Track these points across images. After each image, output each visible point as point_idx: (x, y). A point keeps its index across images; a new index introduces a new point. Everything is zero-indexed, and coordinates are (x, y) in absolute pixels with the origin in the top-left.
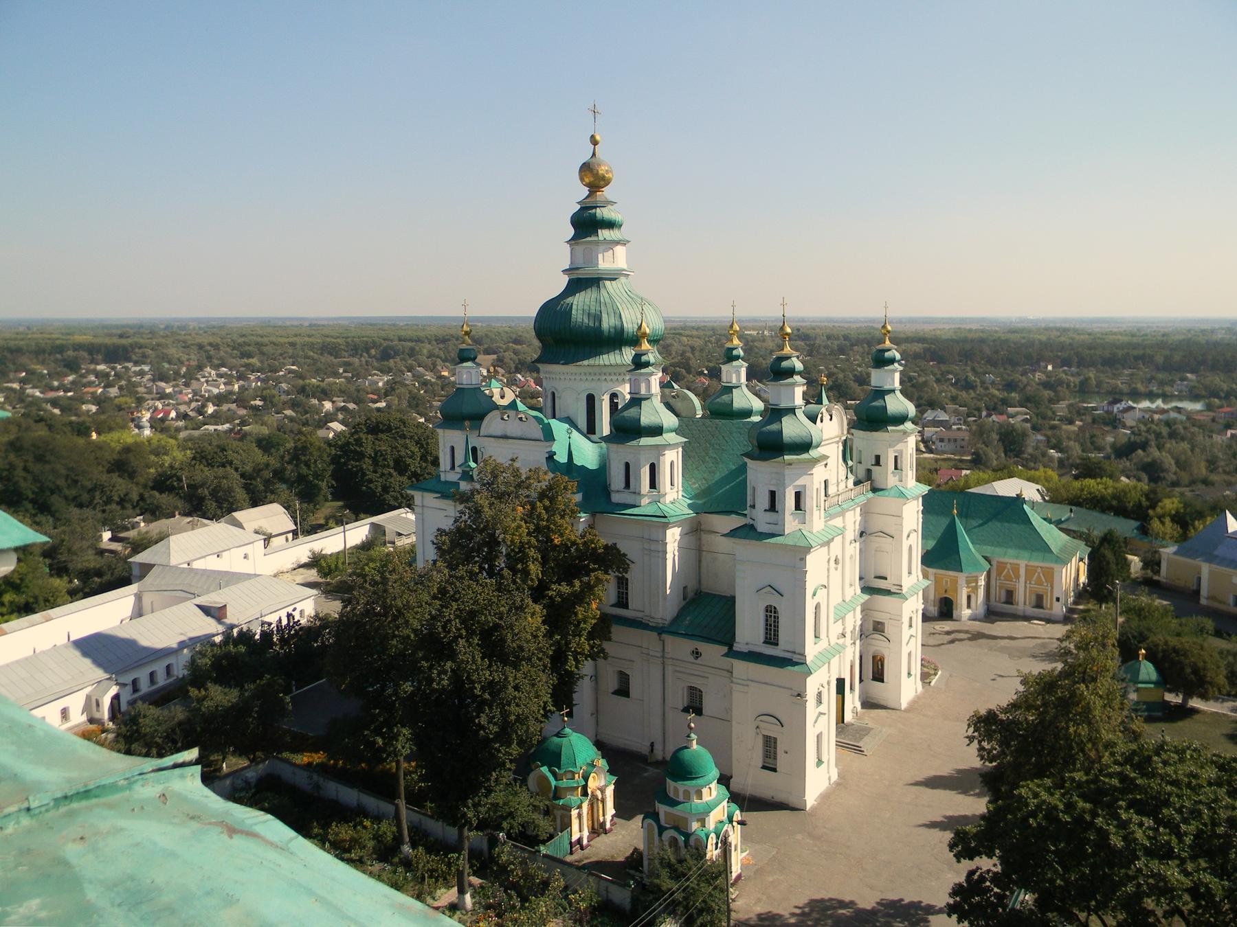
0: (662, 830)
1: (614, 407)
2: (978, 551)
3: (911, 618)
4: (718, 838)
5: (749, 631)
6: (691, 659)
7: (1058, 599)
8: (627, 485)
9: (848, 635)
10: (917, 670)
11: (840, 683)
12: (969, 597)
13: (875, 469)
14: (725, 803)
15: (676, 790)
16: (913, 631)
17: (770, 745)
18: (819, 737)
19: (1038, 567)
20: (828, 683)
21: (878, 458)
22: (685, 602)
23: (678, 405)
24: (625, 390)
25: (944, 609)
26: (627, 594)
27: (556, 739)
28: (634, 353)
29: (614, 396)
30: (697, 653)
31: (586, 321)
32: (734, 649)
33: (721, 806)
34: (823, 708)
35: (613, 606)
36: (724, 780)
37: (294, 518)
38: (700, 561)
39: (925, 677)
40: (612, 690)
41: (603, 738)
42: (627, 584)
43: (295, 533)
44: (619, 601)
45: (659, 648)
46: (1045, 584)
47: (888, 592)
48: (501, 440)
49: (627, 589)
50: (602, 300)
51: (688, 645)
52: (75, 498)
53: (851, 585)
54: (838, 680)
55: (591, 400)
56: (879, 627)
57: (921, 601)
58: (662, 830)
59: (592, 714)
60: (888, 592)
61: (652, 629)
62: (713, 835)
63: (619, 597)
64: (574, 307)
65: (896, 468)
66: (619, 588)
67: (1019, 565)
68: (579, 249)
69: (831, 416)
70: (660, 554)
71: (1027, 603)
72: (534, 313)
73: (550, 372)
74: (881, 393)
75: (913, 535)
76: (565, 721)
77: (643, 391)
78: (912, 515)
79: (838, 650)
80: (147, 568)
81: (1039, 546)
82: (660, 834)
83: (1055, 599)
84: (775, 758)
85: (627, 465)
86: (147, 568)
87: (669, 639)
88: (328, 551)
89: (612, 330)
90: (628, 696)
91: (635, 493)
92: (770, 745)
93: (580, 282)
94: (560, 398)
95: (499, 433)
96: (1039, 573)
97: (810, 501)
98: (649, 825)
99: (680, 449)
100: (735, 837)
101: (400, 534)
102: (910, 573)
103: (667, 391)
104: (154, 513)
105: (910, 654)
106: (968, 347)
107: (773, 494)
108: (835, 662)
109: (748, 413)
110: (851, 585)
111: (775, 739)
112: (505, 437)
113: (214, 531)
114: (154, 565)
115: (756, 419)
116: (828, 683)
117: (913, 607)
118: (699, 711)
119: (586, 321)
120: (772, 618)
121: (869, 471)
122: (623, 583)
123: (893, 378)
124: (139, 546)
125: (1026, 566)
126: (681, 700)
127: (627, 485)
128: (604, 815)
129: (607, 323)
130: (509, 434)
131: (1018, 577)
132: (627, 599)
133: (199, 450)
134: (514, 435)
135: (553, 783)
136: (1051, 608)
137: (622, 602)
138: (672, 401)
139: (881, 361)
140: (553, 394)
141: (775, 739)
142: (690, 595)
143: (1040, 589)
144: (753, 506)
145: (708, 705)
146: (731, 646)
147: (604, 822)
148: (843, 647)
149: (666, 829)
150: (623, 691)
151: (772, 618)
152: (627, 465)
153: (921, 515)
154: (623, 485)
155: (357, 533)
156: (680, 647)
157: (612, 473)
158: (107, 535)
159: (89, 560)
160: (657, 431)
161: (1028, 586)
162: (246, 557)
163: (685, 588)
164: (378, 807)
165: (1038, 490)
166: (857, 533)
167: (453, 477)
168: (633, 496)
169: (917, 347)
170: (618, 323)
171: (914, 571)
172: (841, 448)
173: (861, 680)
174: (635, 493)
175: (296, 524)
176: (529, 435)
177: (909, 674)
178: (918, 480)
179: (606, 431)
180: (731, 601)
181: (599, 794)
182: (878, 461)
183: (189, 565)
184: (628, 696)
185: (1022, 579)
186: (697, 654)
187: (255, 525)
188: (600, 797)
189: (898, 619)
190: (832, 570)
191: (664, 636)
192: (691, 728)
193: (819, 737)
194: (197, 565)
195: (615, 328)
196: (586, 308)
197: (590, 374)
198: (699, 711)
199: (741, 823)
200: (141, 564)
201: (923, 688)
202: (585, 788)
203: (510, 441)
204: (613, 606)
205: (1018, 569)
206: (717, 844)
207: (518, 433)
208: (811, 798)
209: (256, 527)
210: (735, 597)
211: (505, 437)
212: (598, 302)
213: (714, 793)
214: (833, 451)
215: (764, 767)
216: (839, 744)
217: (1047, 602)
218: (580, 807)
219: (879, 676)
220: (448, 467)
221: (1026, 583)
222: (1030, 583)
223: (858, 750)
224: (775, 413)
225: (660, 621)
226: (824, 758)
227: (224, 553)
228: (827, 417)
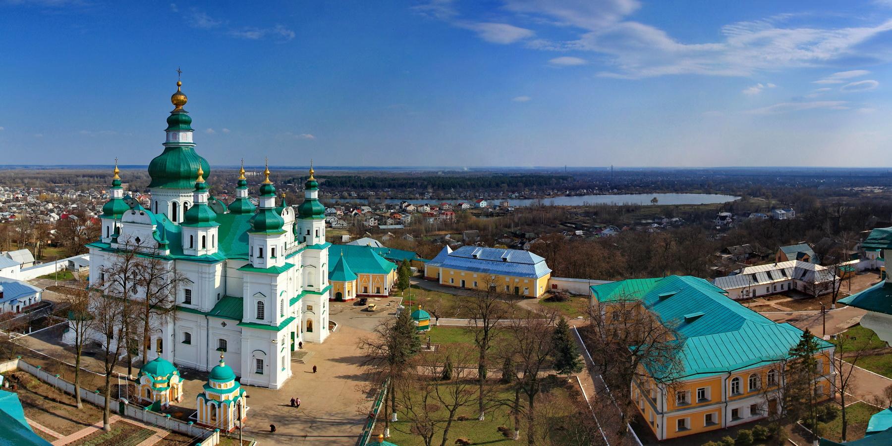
0: (207, 401)
1: (185, 208)
2: (352, 271)
3: (324, 303)
4: (235, 403)
5: (249, 313)
6: (221, 326)
7: (386, 289)
9: (296, 313)
10: (327, 325)
11: (293, 334)
12: (349, 291)
13: (306, 236)
14: (238, 389)
15: (214, 384)
16: (325, 309)
17: (260, 363)
18: (283, 358)
20: (287, 334)
21: (308, 231)
22: (217, 301)
23: (216, 208)
24: (191, 201)
25: (338, 298)
26: (190, 297)
27: (155, 362)
28: (195, 183)
29: (186, 203)
30: (224, 324)
31: (173, 167)
32: (243, 321)
33: (236, 390)
34: (284, 346)
35: (183, 303)
36: (238, 379)
38: (226, 282)
39: (331, 328)
41: (176, 362)
42: (190, 293)
44: (186, 301)
45: (206, 322)
47: (314, 292)
49: (190, 295)
51: (221, 320)
53: (297, 290)
54: (292, 333)
55: (175, 205)
56: (310, 308)
57: (328, 295)
58: (207, 401)
60: (314, 292)
61: (203, 313)
62: (233, 402)
63: (186, 299)
64: (168, 161)
65: (317, 236)
66: (186, 294)
69: (288, 212)
73: (155, 192)
74: (309, 201)
75: (325, 266)
76: (159, 355)
77: (200, 201)
78: (324, 255)
79: (292, 319)
81: (377, 268)
82: (206, 403)
84: (262, 369)
85: (192, 237)
87: (211, 319)
90: (190, 344)
92: (260, 363)
95: (131, 221)
97: (278, 253)
98: (200, 399)
100: (243, 401)
102: (323, 284)
103: (210, 201)
105: (324, 319)
106: (344, 179)
107: (261, 250)
108: (290, 325)
109: (248, 211)
110: (297, 290)
111: (262, 360)
112: (133, 222)
115: (253, 214)
116: (287, 334)
117: (326, 296)
118: (225, 350)
120: (261, 306)
121: (305, 238)
122: (188, 292)
123: (315, 195)
126: (217, 345)
128: (177, 394)
129: (183, 169)
130: (135, 221)
132: (190, 299)
136: (383, 293)
137: (188, 301)
138: (213, 206)
139: (309, 187)
140: (156, 202)
141: (262, 360)
142: (221, 297)
143: (378, 286)
144: (252, 256)
145: (229, 347)
146: (241, 321)
147: (177, 398)
148: (294, 318)
149: (209, 400)
150: (188, 341)
151: (261, 306)
152: (192, 237)
153: (328, 257)
156: (216, 322)
160: (206, 220)
163: (219, 294)
166: (300, 266)
167: (108, 241)
169: (323, 180)
171: (325, 282)
172: (292, 227)
173: (302, 332)
177: (324, 328)
178: (326, 241)
179: (182, 220)
180: (242, 299)
182: (309, 234)
184: (190, 344)
185: (371, 282)
186: (224, 324)
188: (176, 387)
189: (318, 304)
190: (289, 284)
191: (208, 317)
192: (222, 358)
193: (283, 358)
198: (225, 350)
199: (247, 397)
201: (330, 332)
202: (169, 383)
204: (183, 303)
206: (234, 406)
207: (139, 222)
208: (279, 384)
210: (243, 298)
211: (133, 222)
212: (179, 158)
213: (233, 385)
214: (288, 227)
215: (257, 373)
216: (292, 361)
217: (381, 291)
219: (310, 329)
220: (106, 236)
223: (302, 362)
224: (263, 211)
225: (207, 310)
226: (286, 367)
228: (286, 213)
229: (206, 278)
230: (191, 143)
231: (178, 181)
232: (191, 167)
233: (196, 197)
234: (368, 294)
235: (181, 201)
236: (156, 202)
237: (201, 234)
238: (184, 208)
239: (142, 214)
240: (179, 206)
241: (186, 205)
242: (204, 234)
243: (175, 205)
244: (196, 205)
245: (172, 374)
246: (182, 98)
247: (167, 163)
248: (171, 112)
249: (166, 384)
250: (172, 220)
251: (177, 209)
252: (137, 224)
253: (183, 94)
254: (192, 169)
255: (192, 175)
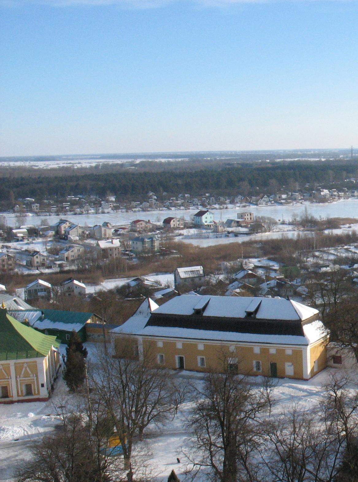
19: (24, 363)
46: (31, 375)
67: (9, 364)
71: (20, 394)
83: (40, 386)
96: (26, 368)
125: (15, 364)
131: (9, 374)
136: (39, 393)
161: (18, 380)
165: (15, 301)
205: (9, 367)
221: (16, 378)
222: (20, 377)
234: (10, 399)
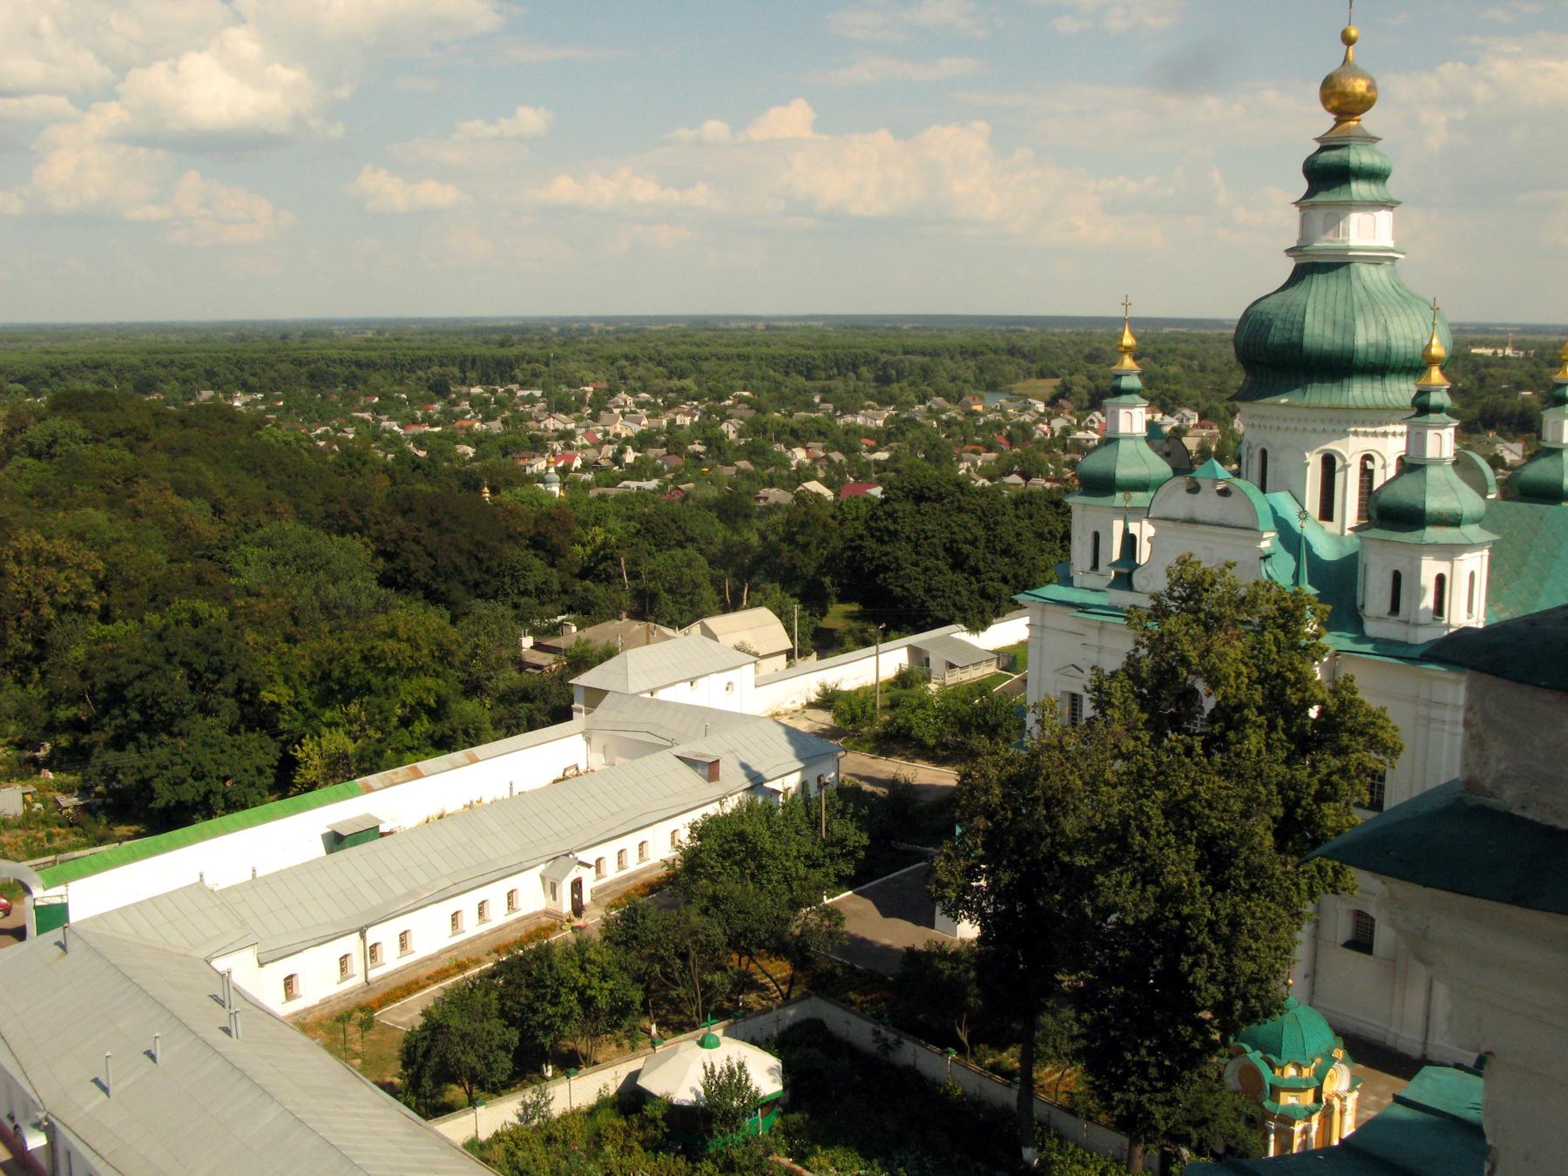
1: (1367, 475)
8: (1395, 608)
37: (789, 629)
40: (1343, 942)
43: (790, 654)
48: (1186, 526)
50: (1355, 299)
52: (477, 585)
55: (1329, 462)
59: (1306, 976)
64: (1309, 310)
68: (1318, 216)
70: (1447, 727)
72: (1238, 315)
80: (595, 697)
86: (595, 697)
88: (846, 686)
89: (1372, 350)
91: (1407, 622)
93: (1309, 268)
94: (1275, 460)
95: (1181, 513)
99: (1486, 552)
101: (952, 666)
104: (587, 612)
112: (1192, 521)
113: (682, 644)
114: (604, 693)
119: (1328, 333)
124: (581, 661)
127: (1395, 608)
133: (643, 519)
134: (1207, 519)
135: (1268, 1076)
140: (1264, 453)
154: (1387, 607)
155: (891, 659)
157: (1370, 588)
158: (527, 642)
159: (508, 678)
162: (728, 687)
164: (980, 1086)
168: (1403, 628)
170: (1382, 339)
174: (1407, 622)
175: (792, 639)
176: (1231, 520)
181: (1336, 1103)
183: (652, 694)
187: (736, 639)
194: (662, 695)
195: (1377, 345)
196: (1340, 317)
197: (1331, 421)
200: (587, 689)
203: (1201, 528)
209: (737, 643)
211: (1192, 521)
212: (1348, 299)
218: (1308, 1119)
227: (700, 680)
229: (1444, 722)
230: (1393, 251)
231: (1346, 382)
232: (1392, 333)
233: (1416, 440)
235: (1351, 449)
236: (1264, 453)
237: (1430, 569)
238: (1362, 475)
239: (1224, 493)
240: (1345, 467)
241: (1369, 465)
242: (1443, 567)
243: (1329, 462)
244: (1410, 466)
245: (1330, 1060)
246: (1360, 86)
247: (1308, 318)
248: (1318, 139)
249: (1310, 1094)
250: (1317, 516)
251: (1339, 477)
252: (1206, 528)
253: (1363, 76)
254: (1394, 343)
255: (1393, 357)
